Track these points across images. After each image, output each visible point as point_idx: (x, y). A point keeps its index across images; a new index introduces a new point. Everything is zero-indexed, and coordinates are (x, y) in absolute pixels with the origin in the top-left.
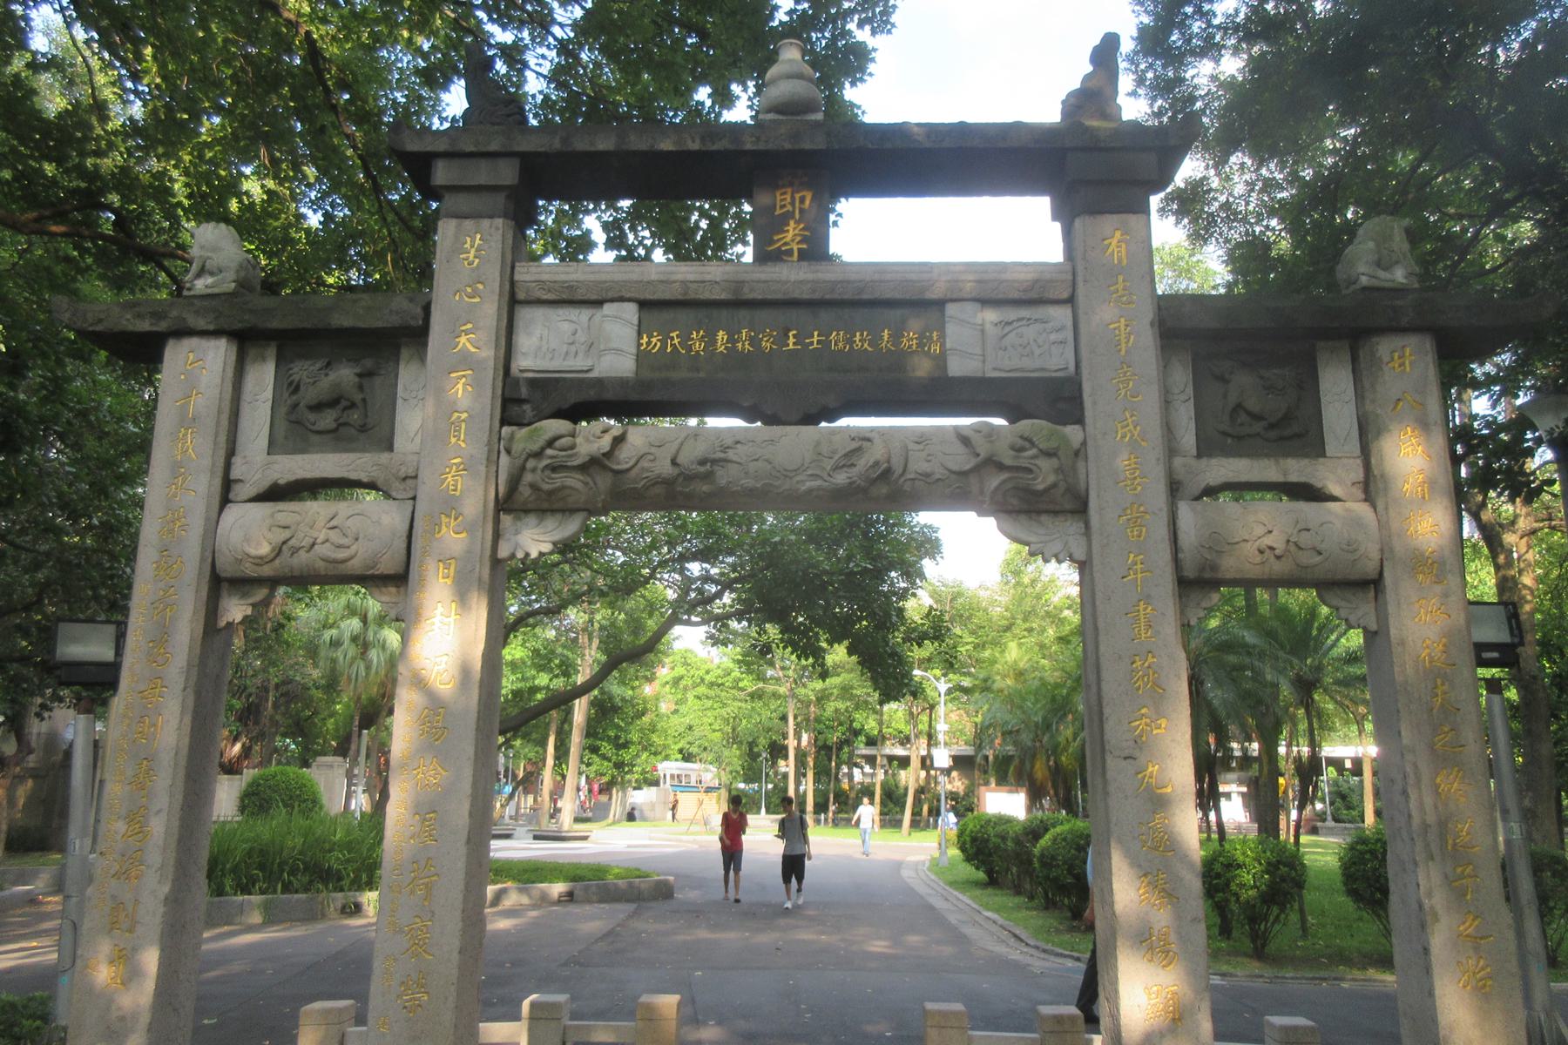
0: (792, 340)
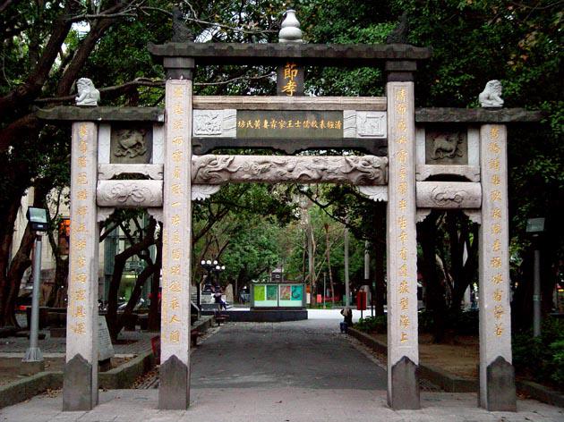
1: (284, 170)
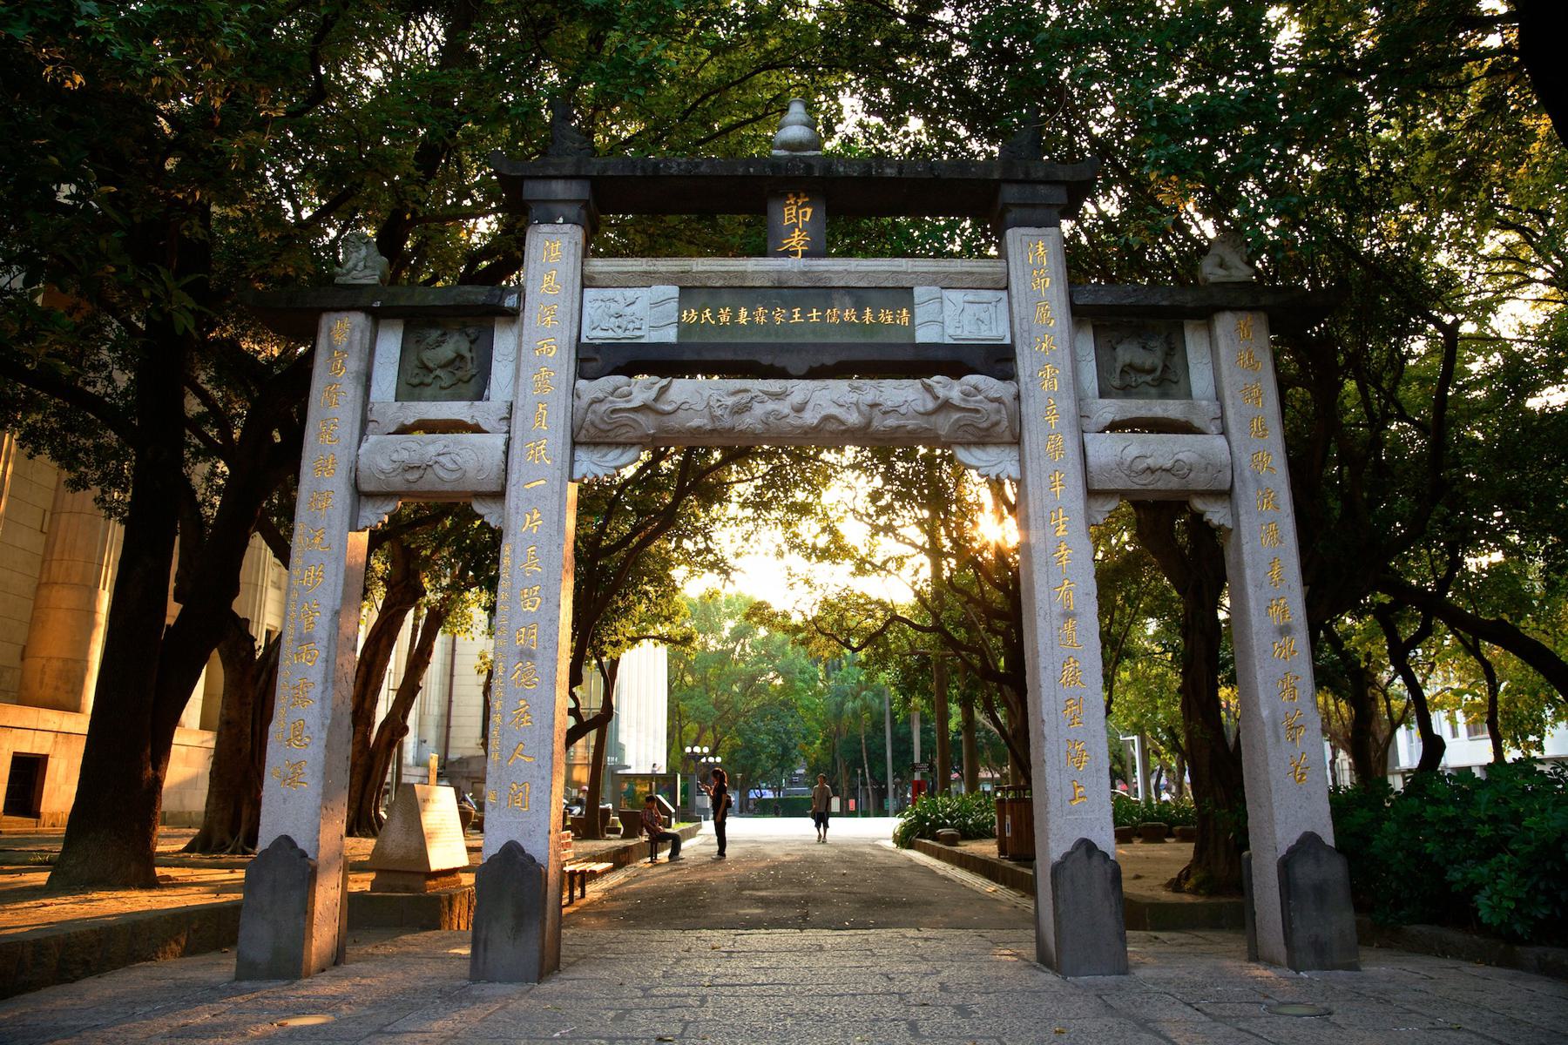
0: (797, 316)
1: (784, 407)
